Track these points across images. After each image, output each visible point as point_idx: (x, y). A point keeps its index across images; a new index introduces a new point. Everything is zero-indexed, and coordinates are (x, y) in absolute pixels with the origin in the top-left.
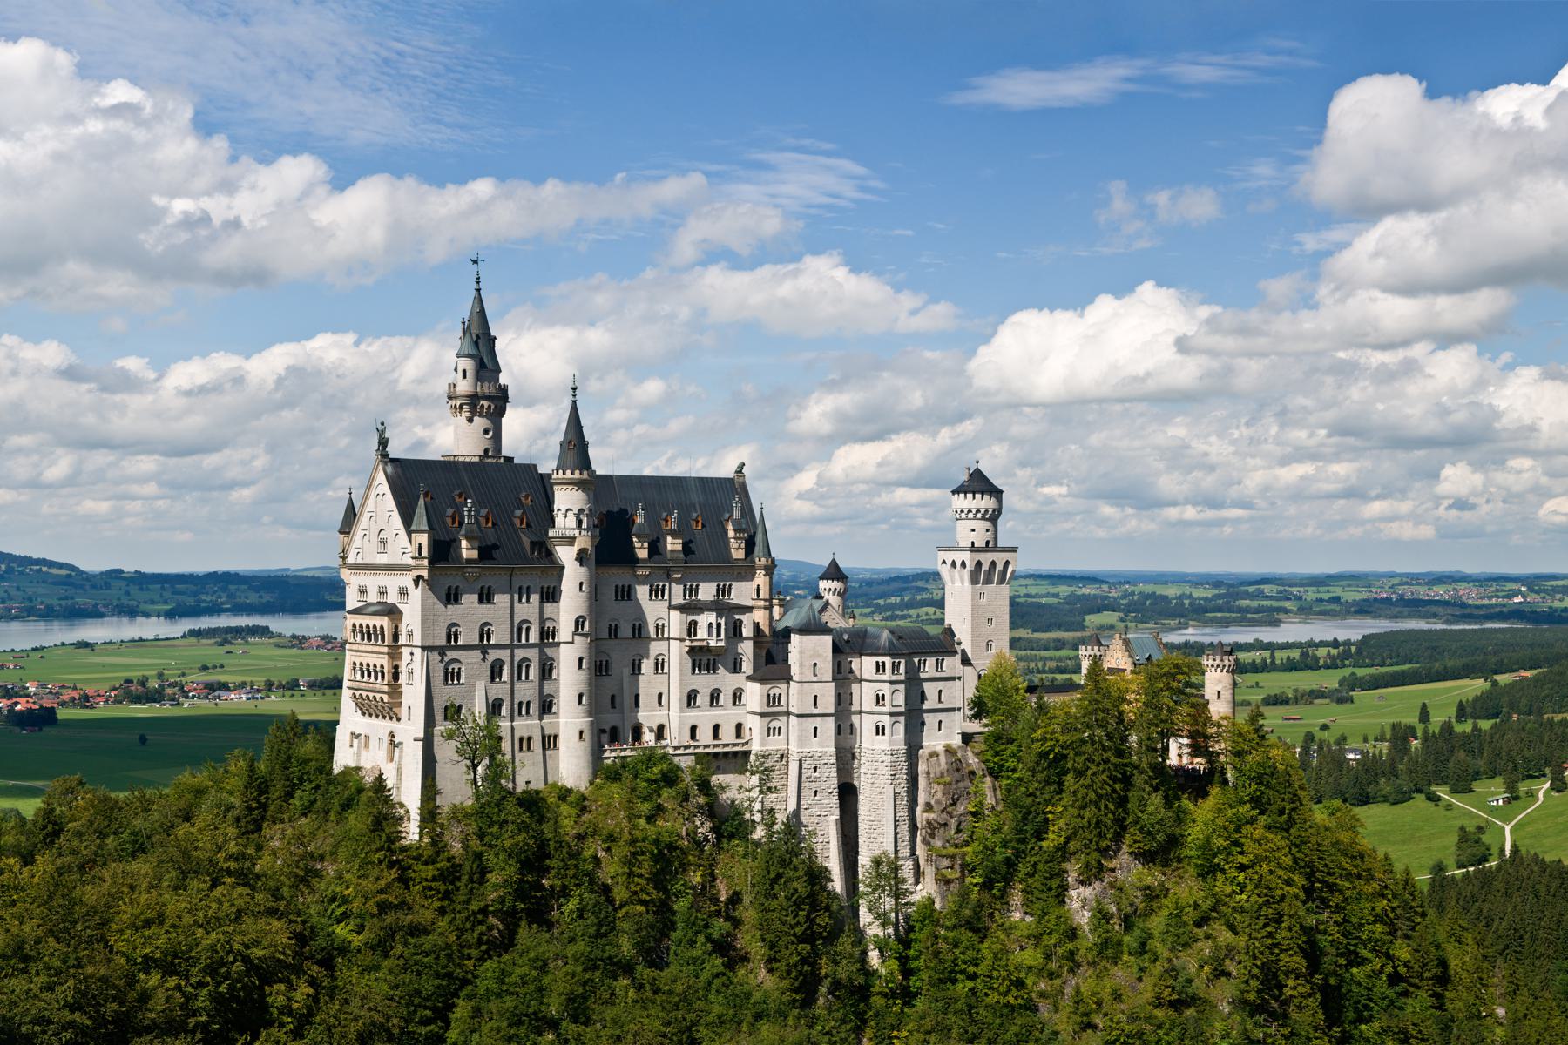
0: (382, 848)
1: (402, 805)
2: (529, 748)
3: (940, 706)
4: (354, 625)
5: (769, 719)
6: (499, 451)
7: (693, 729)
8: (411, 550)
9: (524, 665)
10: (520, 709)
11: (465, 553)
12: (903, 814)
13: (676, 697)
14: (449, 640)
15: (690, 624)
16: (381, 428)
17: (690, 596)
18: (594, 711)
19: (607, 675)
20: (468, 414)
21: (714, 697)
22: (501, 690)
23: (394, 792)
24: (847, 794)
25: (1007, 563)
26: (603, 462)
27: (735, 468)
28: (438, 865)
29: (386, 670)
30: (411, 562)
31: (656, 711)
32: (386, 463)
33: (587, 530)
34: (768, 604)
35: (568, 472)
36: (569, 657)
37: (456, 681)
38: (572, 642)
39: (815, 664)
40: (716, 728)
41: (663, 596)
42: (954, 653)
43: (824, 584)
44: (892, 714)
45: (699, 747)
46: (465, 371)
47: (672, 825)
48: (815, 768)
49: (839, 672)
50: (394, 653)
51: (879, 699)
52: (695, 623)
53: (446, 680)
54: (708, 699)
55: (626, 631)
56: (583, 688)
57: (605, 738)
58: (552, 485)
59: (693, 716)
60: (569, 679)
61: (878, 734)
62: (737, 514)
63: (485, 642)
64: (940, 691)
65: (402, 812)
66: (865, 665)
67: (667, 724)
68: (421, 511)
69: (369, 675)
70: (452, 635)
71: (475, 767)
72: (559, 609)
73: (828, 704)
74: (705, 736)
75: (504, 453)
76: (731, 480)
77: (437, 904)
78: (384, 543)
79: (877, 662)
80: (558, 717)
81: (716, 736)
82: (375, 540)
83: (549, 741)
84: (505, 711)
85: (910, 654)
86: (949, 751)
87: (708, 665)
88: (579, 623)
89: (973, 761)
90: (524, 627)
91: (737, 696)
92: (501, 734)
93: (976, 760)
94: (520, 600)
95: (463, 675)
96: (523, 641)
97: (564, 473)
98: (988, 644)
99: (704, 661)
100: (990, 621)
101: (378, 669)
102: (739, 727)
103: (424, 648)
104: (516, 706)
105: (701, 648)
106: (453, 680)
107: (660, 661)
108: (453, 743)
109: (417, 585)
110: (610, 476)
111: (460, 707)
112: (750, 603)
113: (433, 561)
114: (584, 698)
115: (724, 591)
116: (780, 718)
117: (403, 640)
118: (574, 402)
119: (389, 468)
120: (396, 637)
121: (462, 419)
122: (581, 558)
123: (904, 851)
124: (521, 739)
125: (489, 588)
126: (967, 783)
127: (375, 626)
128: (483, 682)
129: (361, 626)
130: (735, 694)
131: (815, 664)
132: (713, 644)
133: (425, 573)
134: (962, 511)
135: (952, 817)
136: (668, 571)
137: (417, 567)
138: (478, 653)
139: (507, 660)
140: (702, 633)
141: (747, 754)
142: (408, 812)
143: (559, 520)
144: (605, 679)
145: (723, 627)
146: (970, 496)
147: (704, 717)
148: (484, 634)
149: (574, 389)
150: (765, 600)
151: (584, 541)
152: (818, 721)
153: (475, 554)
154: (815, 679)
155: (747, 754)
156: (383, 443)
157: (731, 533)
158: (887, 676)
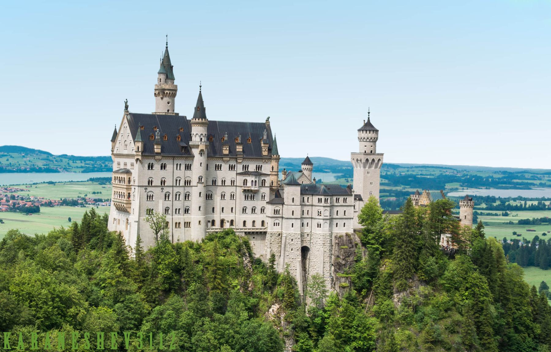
0: (119, 263)
1: (130, 247)
2: (179, 226)
3: (345, 217)
4: (115, 177)
5: (274, 219)
6: (173, 111)
7: (245, 222)
8: (135, 149)
9: (178, 194)
10: (177, 211)
11: (156, 150)
12: (328, 259)
13: (239, 209)
14: (149, 184)
15: (244, 180)
16: (126, 101)
17: (245, 169)
18: (206, 213)
19: (211, 199)
20: (161, 96)
22: (168, 204)
23: (127, 241)
24: (305, 250)
25: (379, 160)
26: (211, 116)
27: (266, 119)
28: (142, 270)
29: (125, 194)
30: (135, 153)
31: (230, 214)
32: (127, 115)
33: (204, 141)
34: (276, 173)
35: (197, 119)
36: (196, 191)
37: (151, 200)
38: (197, 186)
39: (293, 199)
40: (254, 222)
41: (234, 169)
42: (352, 195)
43: (303, 167)
44: (324, 219)
45: (246, 229)
46: (160, 79)
47: (234, 258)
48: (292, 240)
49: (303, 201)
50: (129, 188)
51: (319, 213)
52: (247, 180)
53: (148, 199)
54: (251, 210)
56: (202, 205)
57: (210, 224)
58: (191, 124)
59: (244, 217)
60: (196, 201)
61: (318, 227)
62: (265, 137)
63: (163, 185)
64: (345, 211)
65: (129, 249)
66: (315, 199)
67: (234, 220)
68: (139, 133)
69: (120, 197)
70: (150, 182)
71: (157, 234)
72: (192, 173)
73: (298, 214)
74: (249, 225)
75: (176, 111)
76: (265, 124)
77: (140, 285)
78: (126, 145)
79: (319, 198)
80: (191, 215)
81: (253, 226)
82: (123, 144)
83: (187, 224)
84: (170, 212)
85: (333, 195)
87: (251, 197)
88: (200, 179)
89: (358, 240)
90: (178, 179)
91: (262, 210)
92: (167, 221)
93: (359, 239)
94: (177, 169)
95: (154, 197)
96: (178, 185)
97: (195, 120)
99: (250, 195)
100: (371, 183)
101: (123, 194)
102: (263, 222)
103: (138, 186)
104: (174, 211)
105: (248, 190)
106: (150, 199)
107: (232, 195)
108: (148, 223)
109: (137, 162)
110: (216, 122)
111: (153, 210)
112: (269, 173)
113: (142, 152)
114: (201, 208)
115: (259, 168)
116: (279, 219)
117: (132, 183)
118: (200, 92)
119: (129, 117)
120: (129, 181)
121: (159, 98)
122: (201, 153)
123: (327, 275)
124: (176, 223)
125: (165, 164)
126: (355, 247)
127: (122, 178)
128: (162, 201)
129: (117, 177)
130: (262, 209)
131: (293, 199)
132: (253, 189)
133: (140, 158)
134: (361, 138)
135: (347, 262)
136: (236, 158)
137: (137, 155)
138: (159, 189)
139: (171, 192)
140: (249, 184)
141: (265, 233)
142: (132, 249)
143: (193, 138)
144: (210, 201)
145: (257, 182)
146: (365, 132)
147: (249, 217)
148: (163, 182)
149: (200, 86)
150: (275, 172)
151: (202, 147)
152: (294, 221)
154: (293, 204)
155: (265, 233)
156: (127, 107)
157: (262, 145)
158: (323, 204)
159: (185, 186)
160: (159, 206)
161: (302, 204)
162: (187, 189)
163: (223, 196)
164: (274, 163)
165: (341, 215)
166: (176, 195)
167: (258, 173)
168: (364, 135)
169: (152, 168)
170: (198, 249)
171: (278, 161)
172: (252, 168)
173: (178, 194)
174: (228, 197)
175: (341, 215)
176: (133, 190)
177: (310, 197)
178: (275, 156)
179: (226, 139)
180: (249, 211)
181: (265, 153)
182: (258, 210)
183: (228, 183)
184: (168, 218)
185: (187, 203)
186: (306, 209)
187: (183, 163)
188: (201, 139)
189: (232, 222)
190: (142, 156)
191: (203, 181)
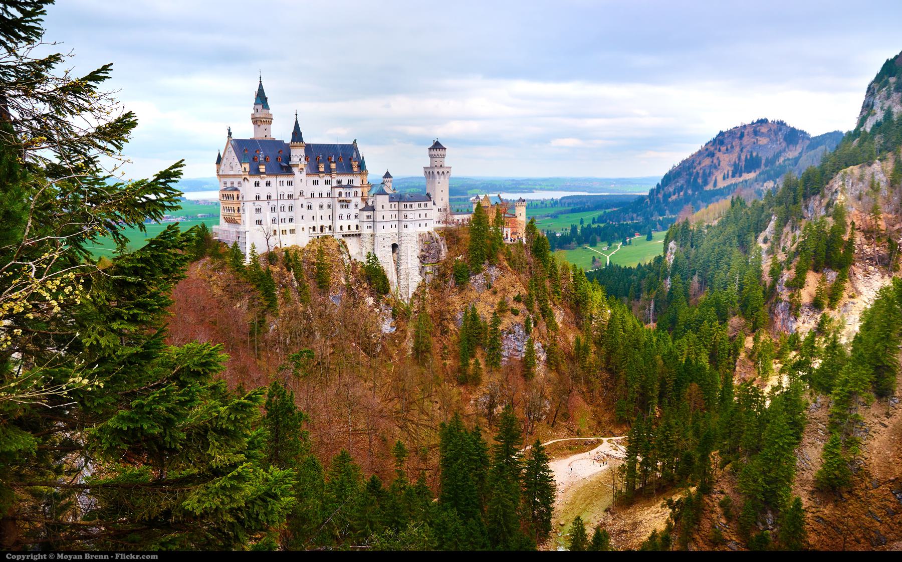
7: (341, 227)
10: (283, 220)
11: (261, 170)
21: (348, 217)
40: (349, 226)
55: (317, 195)
57: (311, 230)
62: (354, 156)
70: (258, 198)
74: (345, 229)
78: (232, 167)
84: (276, 221)
86: (429, 233)
88: (301, 194)
98: (442, 200)
102: (357, 226)
115: (351, 182)
117: (240, 199)
120: (238, 198)
132: (348, 199)
133: (247, 177)
140: (344, 195)
147: (345, 223)
148: (269, 197)
152: (384, 224)
155: (360, 235)
158: (408, 208)
160: (267, 216)
163: (321, 207)
165: (423, 217)
167: (350, 185)
168: (434, 152)
172: (345, 183)
174: (325, 206)
175: (423, 217)
176: (242, 205)
177: (397, 203)
179: (321, 158)
180: (345, 217)
181: (355, 169)
182: (353, 217)
183: (325, 195)
184: (275, 227)
185: (291, 214)
186: (393, 213)
187: (285, 179)
189: (330, 228)
190: (250, 175)
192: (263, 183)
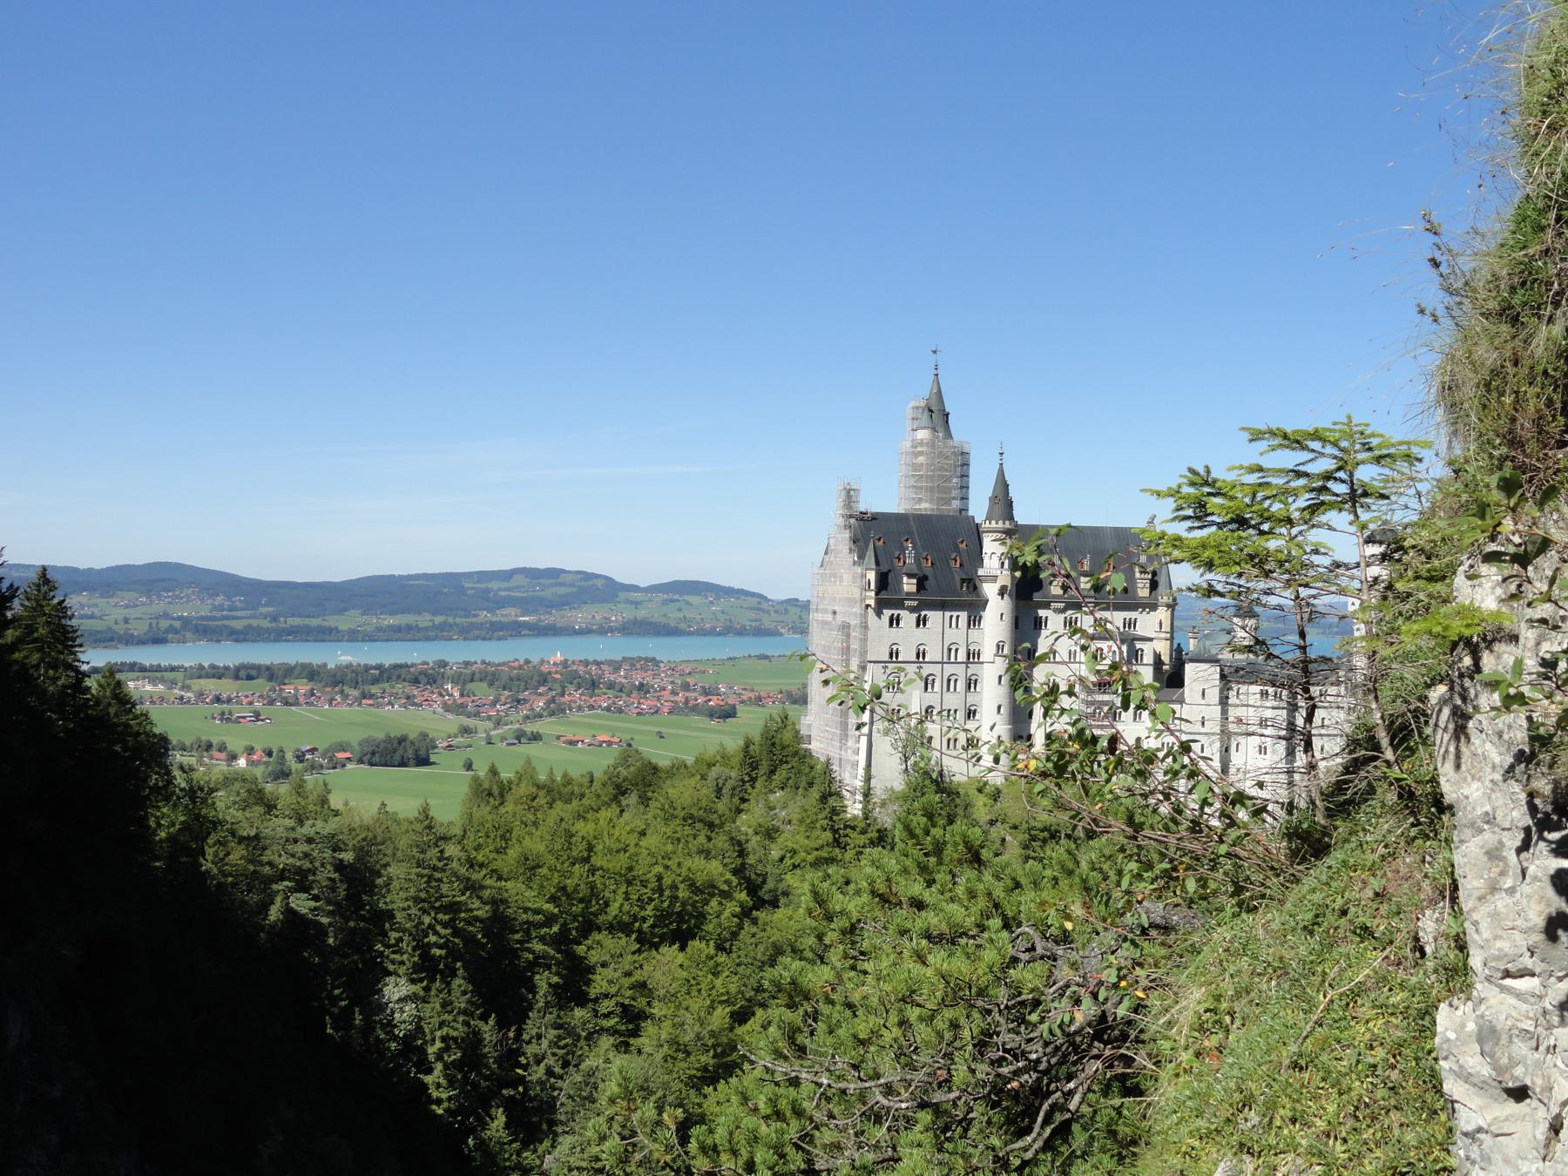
14: (891, 657)
22: (932, 698)
26: (1022, 516)
28: (869, 835)
36: (992, 674)
56: (1005, 702)
68: (870, 554)
70: (894, 654)
88: (999, 647)
96: (953, 660)
115: (1131, 624)
133: (872, 603)
143: (986, 561)
148: (920, 654)
151: (1005, 578)
153: (913, 588)
157: (1138, 575)
159: (967, 663)
161: (1224, 702)
162: (973, 669)
164: (1162, 614)
166: (949, 681)
169: (898, 624)
170: (996, 795)
171: (1173, 610)
173: (953, 678)
178: (1165, 598)
184: (932, 729)
185: (971, 699)
188: (1003, 564)
191: (1006, 651)
192: (908, 618)
